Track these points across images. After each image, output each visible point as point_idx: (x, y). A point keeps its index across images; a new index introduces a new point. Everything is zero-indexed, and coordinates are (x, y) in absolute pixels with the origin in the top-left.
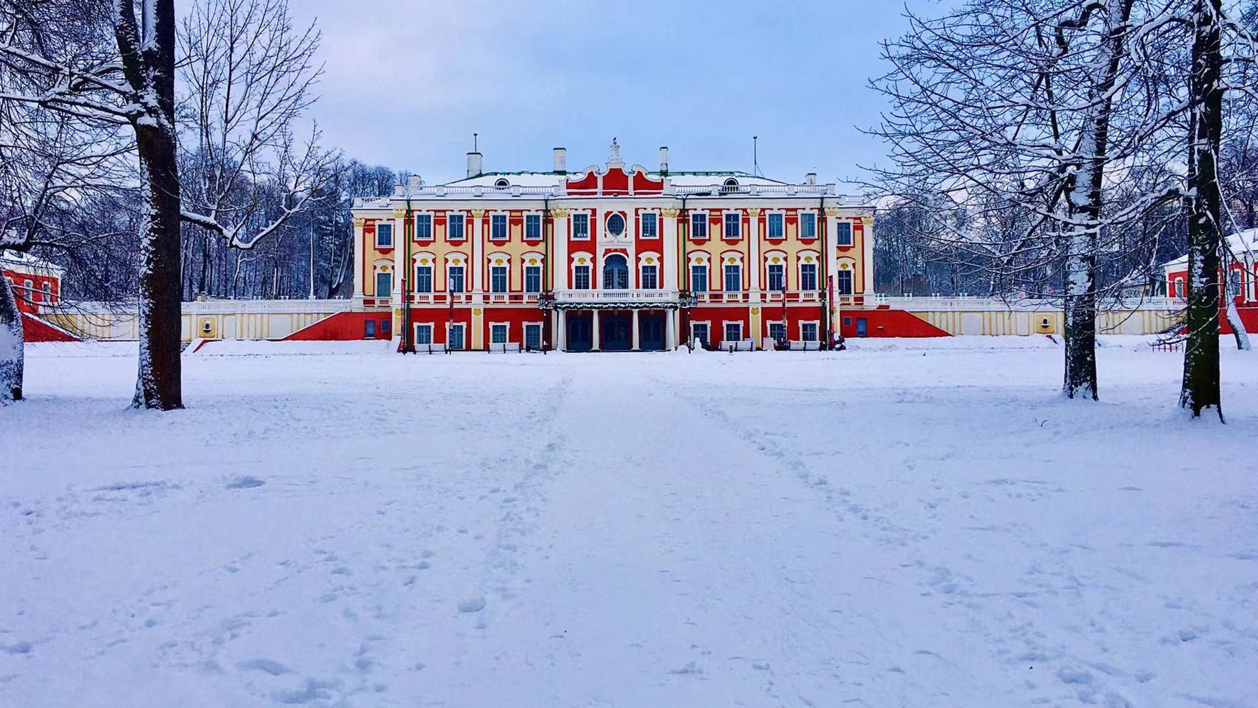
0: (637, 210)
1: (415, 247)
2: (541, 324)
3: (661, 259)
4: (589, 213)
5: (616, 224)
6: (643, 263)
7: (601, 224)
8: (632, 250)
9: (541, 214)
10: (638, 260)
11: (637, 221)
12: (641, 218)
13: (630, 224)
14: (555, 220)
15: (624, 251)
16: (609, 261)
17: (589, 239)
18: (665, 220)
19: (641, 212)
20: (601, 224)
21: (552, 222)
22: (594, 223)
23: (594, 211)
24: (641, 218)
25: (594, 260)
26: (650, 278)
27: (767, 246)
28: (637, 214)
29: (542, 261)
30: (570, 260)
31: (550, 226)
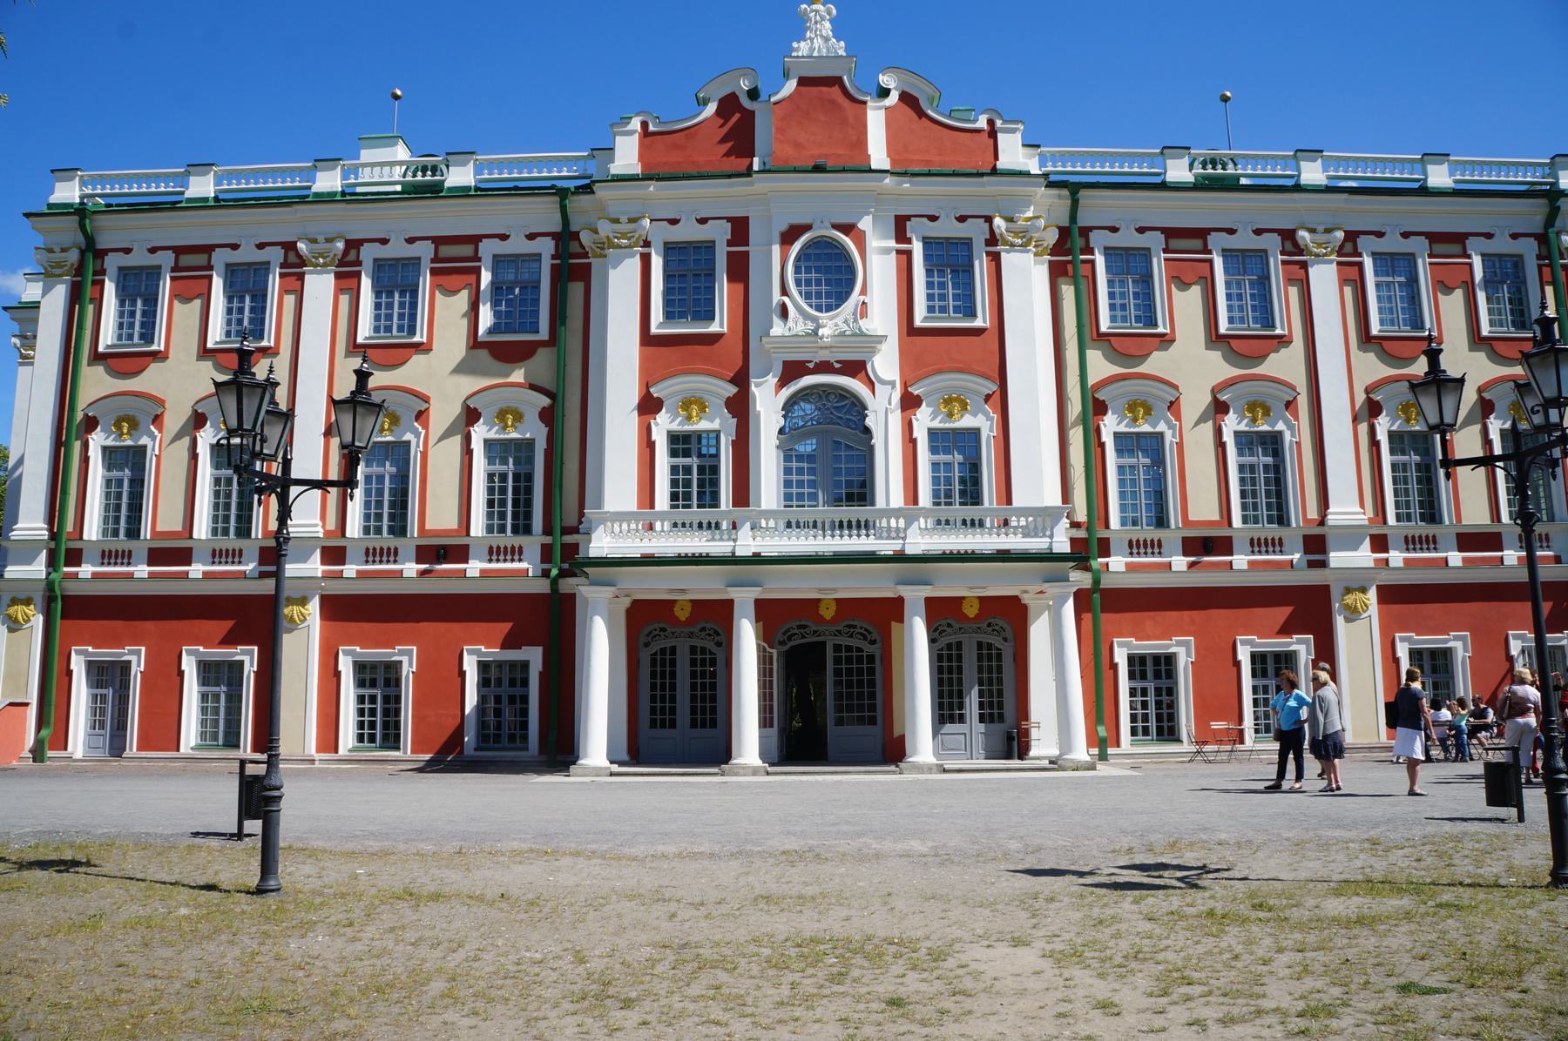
1: (95, 384)
2: (533, 656)
3: (1000, 401)
4: (720, 233)
8: (886, 364)
9: (546, 247)
10: (910, 403)
18: (1009, 260)
21: (584, 274)
23: (740, 229)
24: (917, 248)
25: (740, 407)
26: (966, 475)
29: (547, 416)
30: (649, 406)
31: (576, 289)
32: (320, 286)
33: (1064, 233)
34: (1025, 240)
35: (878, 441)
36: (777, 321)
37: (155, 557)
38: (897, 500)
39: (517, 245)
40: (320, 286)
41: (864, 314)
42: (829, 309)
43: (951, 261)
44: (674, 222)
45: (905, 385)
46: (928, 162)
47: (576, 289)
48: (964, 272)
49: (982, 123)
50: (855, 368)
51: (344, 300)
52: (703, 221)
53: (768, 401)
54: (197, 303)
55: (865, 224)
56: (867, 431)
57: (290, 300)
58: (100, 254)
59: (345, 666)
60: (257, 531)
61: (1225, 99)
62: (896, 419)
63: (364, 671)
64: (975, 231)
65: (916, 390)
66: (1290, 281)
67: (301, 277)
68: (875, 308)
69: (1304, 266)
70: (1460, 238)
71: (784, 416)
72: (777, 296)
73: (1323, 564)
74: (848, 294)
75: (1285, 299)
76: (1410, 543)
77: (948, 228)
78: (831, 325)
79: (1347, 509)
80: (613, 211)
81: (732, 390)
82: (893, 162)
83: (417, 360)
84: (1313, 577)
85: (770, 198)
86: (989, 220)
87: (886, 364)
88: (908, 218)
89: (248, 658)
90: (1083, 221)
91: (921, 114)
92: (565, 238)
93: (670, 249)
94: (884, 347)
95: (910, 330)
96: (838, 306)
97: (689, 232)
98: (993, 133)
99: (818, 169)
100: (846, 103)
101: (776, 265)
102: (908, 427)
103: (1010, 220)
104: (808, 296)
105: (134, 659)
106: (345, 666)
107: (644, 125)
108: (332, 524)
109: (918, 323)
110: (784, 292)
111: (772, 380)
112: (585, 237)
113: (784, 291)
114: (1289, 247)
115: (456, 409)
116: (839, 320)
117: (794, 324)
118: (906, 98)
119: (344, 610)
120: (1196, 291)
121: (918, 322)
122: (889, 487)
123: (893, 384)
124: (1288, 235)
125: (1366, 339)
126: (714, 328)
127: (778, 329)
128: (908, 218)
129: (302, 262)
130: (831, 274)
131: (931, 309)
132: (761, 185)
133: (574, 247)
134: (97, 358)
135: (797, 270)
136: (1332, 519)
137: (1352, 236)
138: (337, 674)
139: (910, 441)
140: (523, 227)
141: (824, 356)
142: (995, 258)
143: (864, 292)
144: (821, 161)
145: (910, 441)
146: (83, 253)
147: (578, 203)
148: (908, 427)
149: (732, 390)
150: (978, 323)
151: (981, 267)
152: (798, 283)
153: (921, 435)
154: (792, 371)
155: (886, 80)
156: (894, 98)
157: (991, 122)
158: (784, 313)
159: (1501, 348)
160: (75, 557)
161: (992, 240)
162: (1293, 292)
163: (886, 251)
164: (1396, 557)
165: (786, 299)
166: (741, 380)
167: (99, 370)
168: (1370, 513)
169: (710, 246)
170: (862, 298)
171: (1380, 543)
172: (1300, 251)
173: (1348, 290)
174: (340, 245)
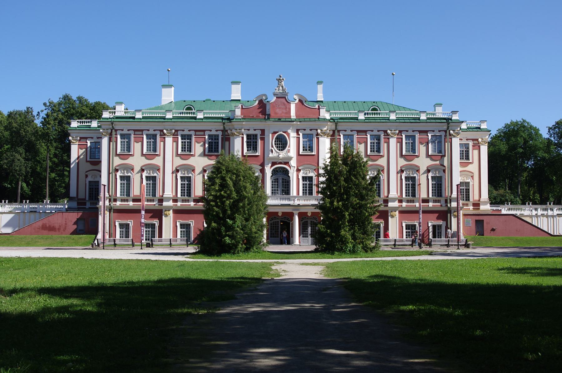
1: (117, 161)
4: (258, 133)
8: (293, 163)
9: (220, 133)
10: (298, 170)
14: (231, 138)
15: (287, 163)
16: (275, 172)
18: (321, 139)
21: (228, 139)
23: (263, 131)
24: (301, 136)
25: (263, 171)
27: (402, 162)
31: (227, 143)
32: (169, 140)
33: (334, 131)
34: (324, 134)
35: (291, 179)
36: (270, 153)
37: (134, 200)
38: (295, 194)
39: (214, 133)
40: (169, 140)
41: (289, 152)
42: (282, 150)
43: (309, 138)
44: (249, 130)
45: (297, 167)
47: (227, 143)
48: (311, 141)
49: (317, 107)
50: (287, 163)
51: (175, 143)
52: (255, 130)
53: (269, 170)
54: (140, 143)
55: (289, 131)
56: (289, 176)
57: (162, 143)
58: (116, 130)
59: (178, 224)
60: (157, 195)
61: (393, 74)
62: (295, 173)
63: (182, 226)
64: (314, 132)
65: (300, 168)
66: (385, 142)
67: (165, 138)
69: (389, 139)
70: (426, 132)
72: (271, 148)
73: (387, 206)
74: (286, 147)
75: (384, 146)
76: (408, 201)
77: (308, 132)
78: (282, 154)
79: (394, 193)
80: (236, 127)
81: (261, 168)
83: (192, 158)
84: (385, 209)
85: (270, 126)
86: (317, 130)
87: (293, 163)
88: (299, 130)
89: (156, 222)
90: (339, 128)
91: (303, 104)
92: (224, 131)
93: (248, 136)
95: (299, 154)
97: (252, 132)
98: (319, 109)
100: (286, 103)
101: (271, 140)
102: (298, 176)
103: (321, 130)
104: (277, 147)
105: (130, 223)
106: (178, 224)
107: (242, 106)
108: (174, 194)
109: (300, 153)
110: (272, 147)
111: (270, 165)
112: (229, 132)
113: (272, 147)
114: (386, 134)
115: (201, 169)
117: (274, 153)
118: (300, 100)
119: (178, 212)
120: (363, 144)
121: (300, 153)
124: (385, 132)
125: (402, 156)
126: (257, 154)
127: (271, 155)
128: (299, 130)
129: (165, 134)
130: (282, 143)
132: (268, 123)
133: (226, 133)
134: (117, 155)
135: (275, 141)
136: (390, 196)
137: (400, 132)
138: (177, 226)
139: (298, 179)
140: (215, 128)
141: (280, 161)
142: (318, 138)
145: (298, 179)
146: (112, 130)
147: (228, 125)
148: (298, 176)
149: (261, 168)
150: (313, 153)
151: (315, 140)
154: (273, 164)
155: (296, 97)
156: (297, 101)
157: (319, 106)
158: (272, 151)
159: (433, 157)
160: (115, 200)
161: (317, 134)
162: (386, 144)
163: (294, 137)
164: (404, 204)
166: (263, 165)
167: (118, 158)
168: (399, 195)
169: (256, 135)
171: (400, 201)
172: (388, 135)
173: (398, 144)
174: (174, 131)
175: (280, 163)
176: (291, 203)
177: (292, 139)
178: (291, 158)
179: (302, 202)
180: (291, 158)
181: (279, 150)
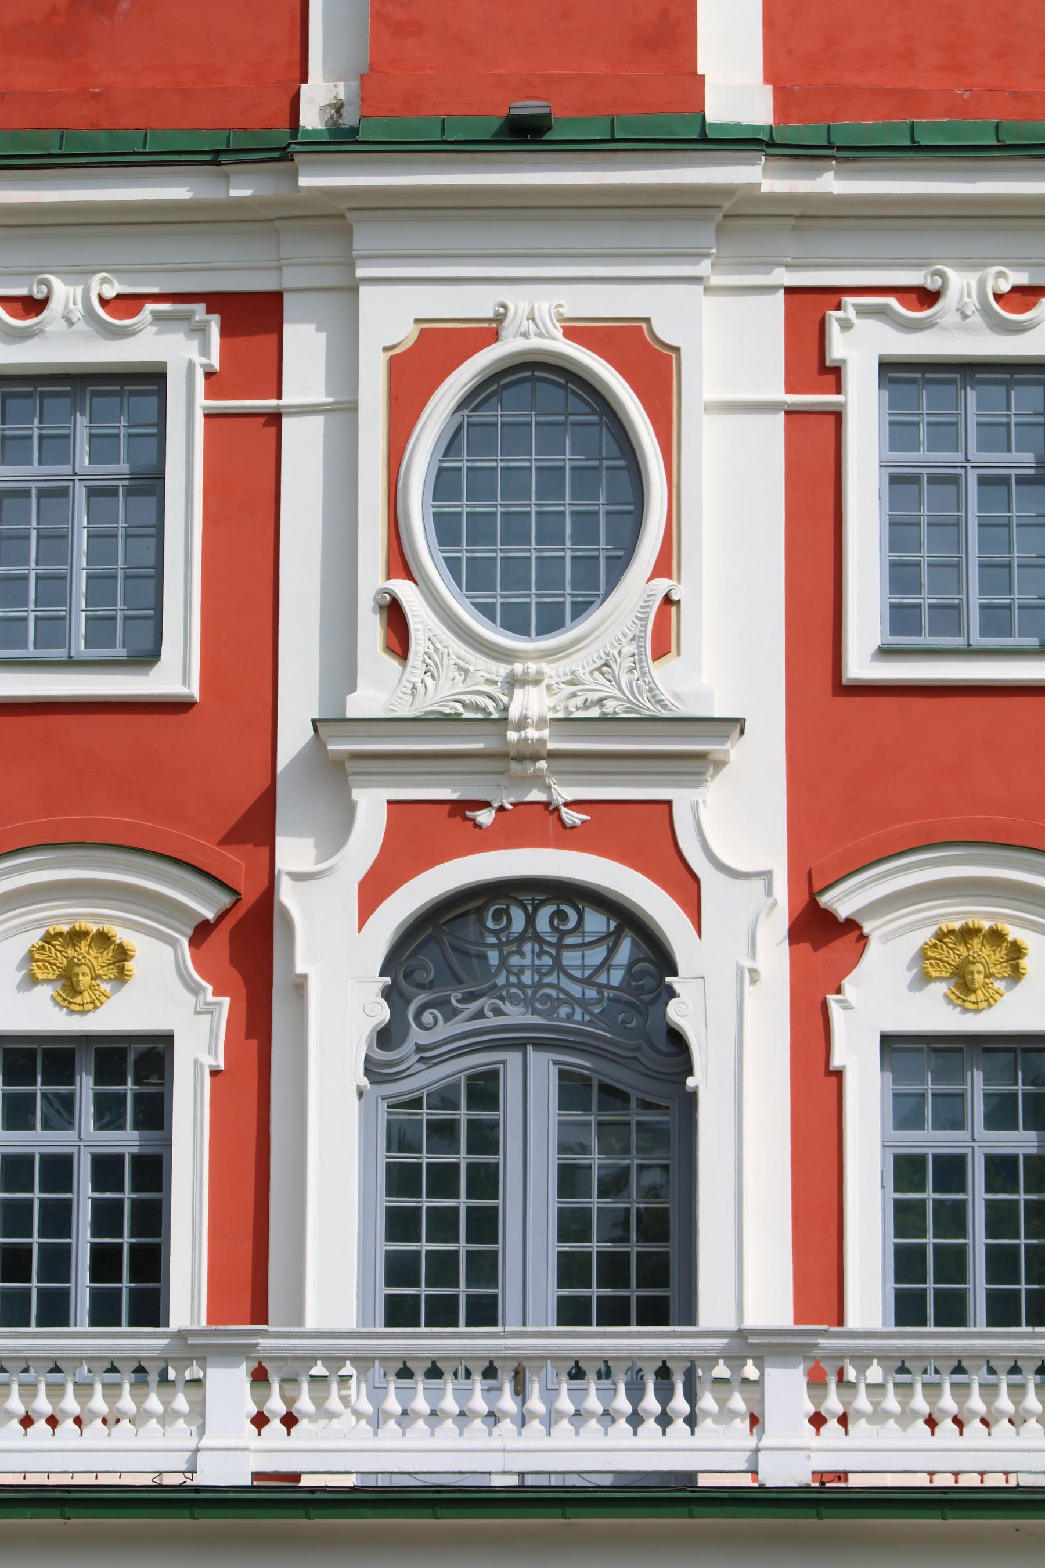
0: (809, 312)
5: (552, 471)
6: (883, 996)
7: (351, 479)
8: (739, 819)
11: (815, 450)
12: (863, 403)
13: (721, 488)
15: (648, 836)
16: (434, 954)
17: (176, 673)
19: (859, 344)
20: (351, 479)
22: (246, 455)
24: (863, 403)
25: (247, 948)
28: (811, 362)
35: (707, 1079)
41: (662, 643)
42: (552, 621)
46: (908, 98)
65: (843, 901)
68: (702, 624)
71: (388, 994)
74: (619, 565)
78: (552, 683)
82: (785, 100)
94: (736, 751)
96: (581, 609)
99: (525, 134)
109: (861, 665)
110: (400, 563)
113: (400, 563)
116: (581, 663)
121: (861, 665)
122: (743, 1259)
123: (766, 875)
128: (835, 294)
131: (901, 618)
135: (444, 484)
143: (663, 567)
144: (528, 106)
152: (445, 529)
153: (856, 1054)
165: (405, 590)
170: (662, 585)
175: (539, 824)
176: (712, 1450)
177: (704, 436)
178: (693, 744)
179: (889, 1448)
180: (693, 744)
181: (515, 621)
